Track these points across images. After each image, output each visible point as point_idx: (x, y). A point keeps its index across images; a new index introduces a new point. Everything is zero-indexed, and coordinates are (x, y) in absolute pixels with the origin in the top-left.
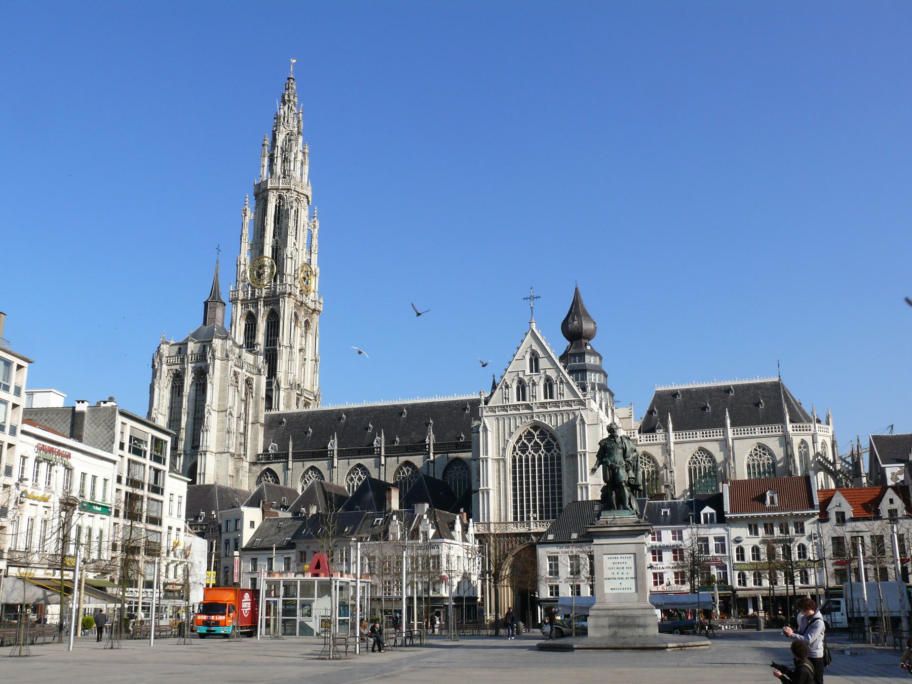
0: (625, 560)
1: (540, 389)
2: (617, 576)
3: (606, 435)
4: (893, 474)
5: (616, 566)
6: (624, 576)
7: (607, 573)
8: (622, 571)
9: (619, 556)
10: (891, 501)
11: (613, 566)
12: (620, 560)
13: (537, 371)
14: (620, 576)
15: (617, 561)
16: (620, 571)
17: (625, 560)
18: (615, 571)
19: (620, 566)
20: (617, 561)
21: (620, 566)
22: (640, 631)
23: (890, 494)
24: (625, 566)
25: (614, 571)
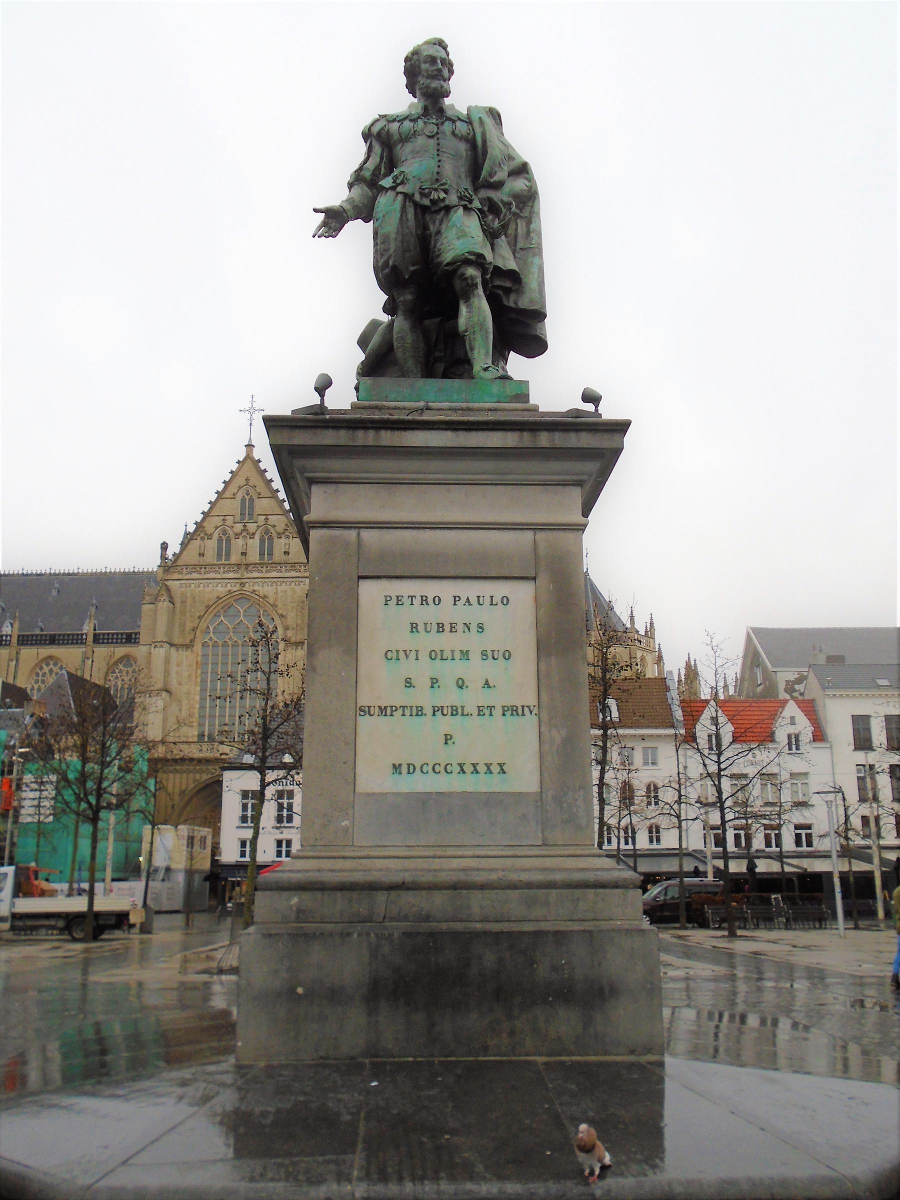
0: (475, 615)
1: (254, 544)
2: (424, 697)
3: (400, 101)
4: (788, 682)
5: (428, 641)
6: (471, 699)
7: (378, 682)
8: (458, 668)
9: (446, 590)
10: (793, 721)
11: (405, 640)
12: (447, 613)
13: (251, 518)
14: (449, 696)
15: (431, 614)
16: (449, 671)
17: (475, 615)
18: (421, 670)
19: (446, 642)
20: (431, 614)
21: (446, 642)
22: (565, 1022)
23: (791, 709)
24: (474, 642)
25: (408, 668)
